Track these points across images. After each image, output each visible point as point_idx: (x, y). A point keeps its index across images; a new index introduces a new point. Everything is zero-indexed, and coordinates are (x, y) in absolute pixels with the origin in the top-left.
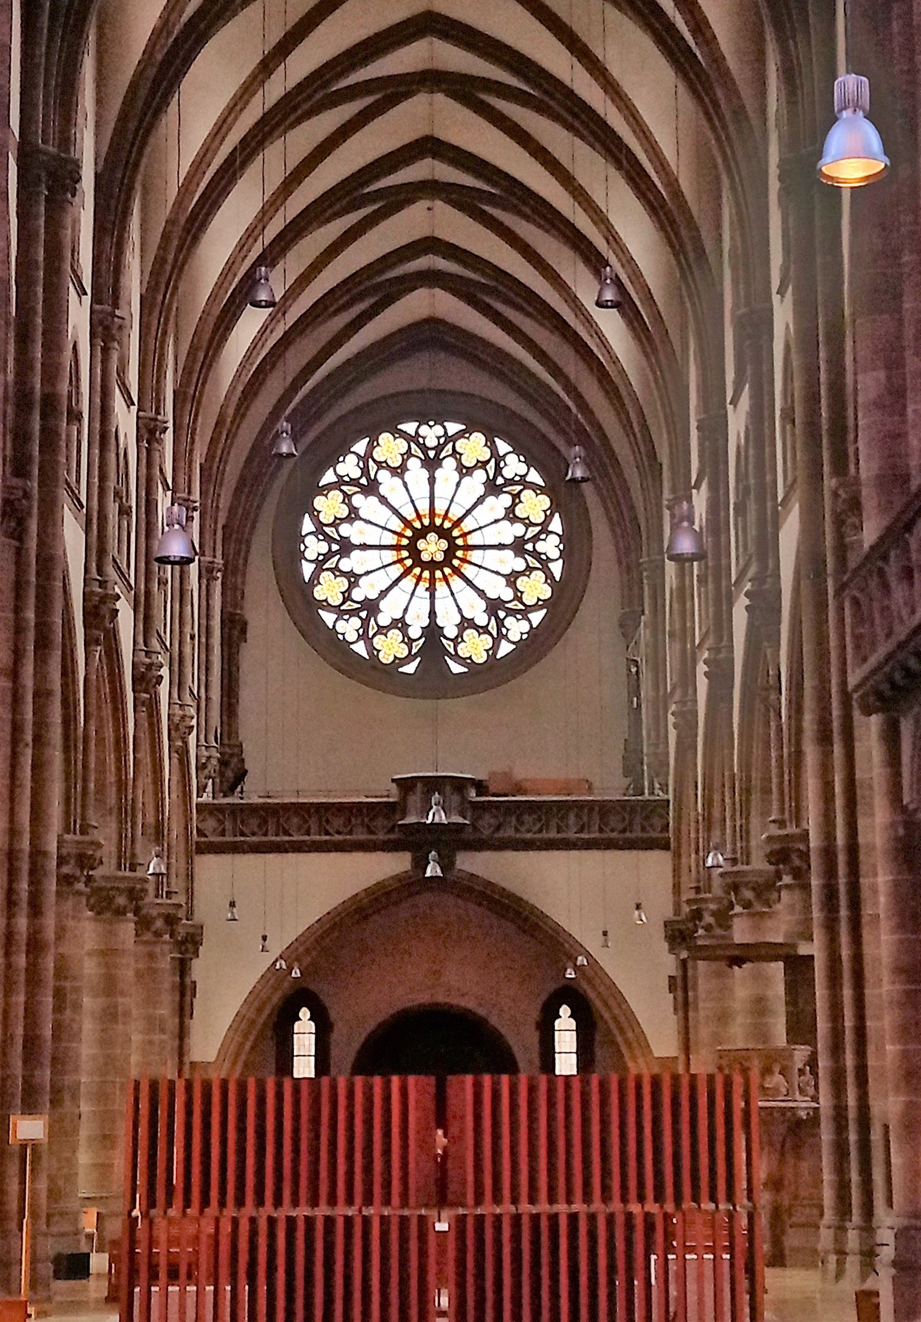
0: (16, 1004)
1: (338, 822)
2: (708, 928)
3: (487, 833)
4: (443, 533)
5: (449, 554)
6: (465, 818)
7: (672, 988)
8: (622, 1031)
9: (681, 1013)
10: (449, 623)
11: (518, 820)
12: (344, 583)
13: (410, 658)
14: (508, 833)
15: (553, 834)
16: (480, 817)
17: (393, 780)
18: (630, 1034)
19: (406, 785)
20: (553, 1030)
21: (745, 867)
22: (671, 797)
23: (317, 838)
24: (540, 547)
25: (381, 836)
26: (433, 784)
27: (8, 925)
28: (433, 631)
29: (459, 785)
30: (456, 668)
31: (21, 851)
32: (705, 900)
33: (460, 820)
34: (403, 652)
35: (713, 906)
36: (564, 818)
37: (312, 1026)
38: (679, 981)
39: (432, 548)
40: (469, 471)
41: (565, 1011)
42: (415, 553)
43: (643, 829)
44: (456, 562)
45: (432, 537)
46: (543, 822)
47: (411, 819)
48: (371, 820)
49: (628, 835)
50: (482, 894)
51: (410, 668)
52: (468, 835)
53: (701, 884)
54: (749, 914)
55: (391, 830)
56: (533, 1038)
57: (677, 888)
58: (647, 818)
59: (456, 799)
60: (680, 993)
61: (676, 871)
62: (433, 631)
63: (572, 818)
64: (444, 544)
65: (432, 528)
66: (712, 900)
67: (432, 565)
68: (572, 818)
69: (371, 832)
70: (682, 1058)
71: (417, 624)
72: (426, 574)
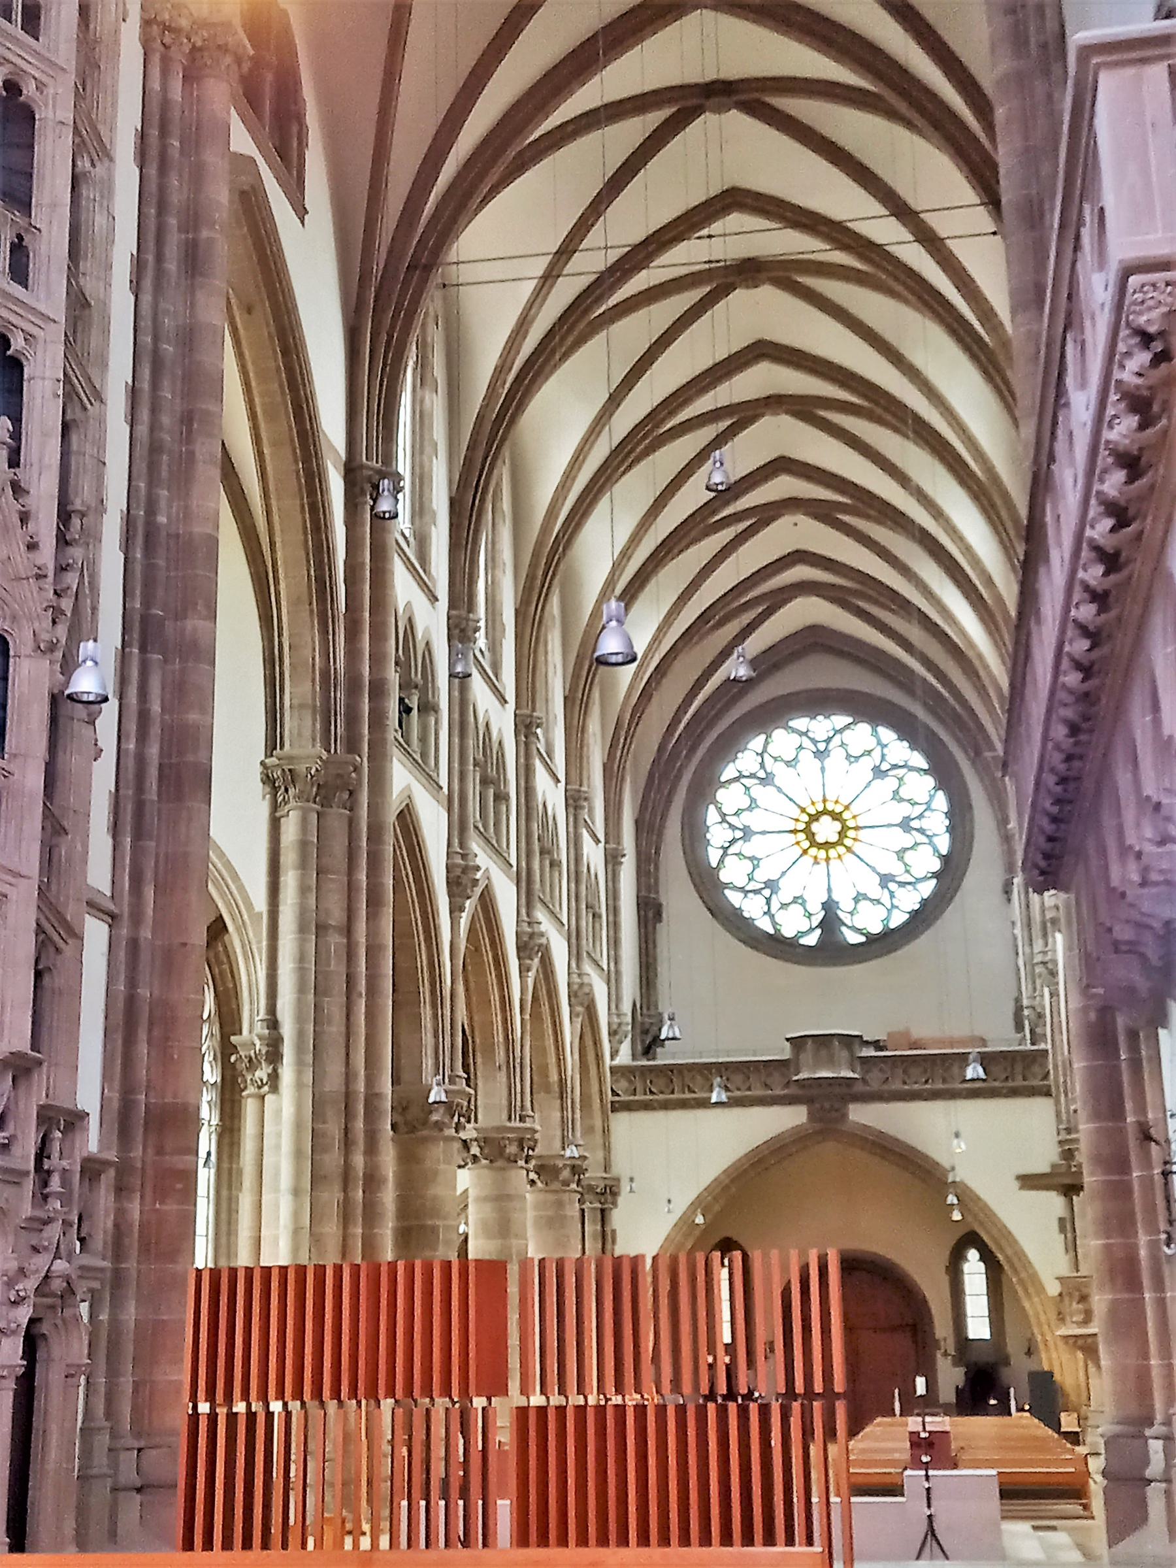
3: (875, 1085)
11: (905, 1072)
14: (896, 1085)
15: (940, 1086)
16: (867, 1072)
17: (788, 1040)
19: (797, 1043)
25: (779, 1092)
26: (823, 1041)
29: (848, 1041)
33: (851, 1075)
36: (947, 1069)
46: (928, 1075)
47: (803, 1075)
48: (770, 1075)
50: (874, 1143)
52: (859, 1088)
55: (788, 1084)
59: (845, 1054)
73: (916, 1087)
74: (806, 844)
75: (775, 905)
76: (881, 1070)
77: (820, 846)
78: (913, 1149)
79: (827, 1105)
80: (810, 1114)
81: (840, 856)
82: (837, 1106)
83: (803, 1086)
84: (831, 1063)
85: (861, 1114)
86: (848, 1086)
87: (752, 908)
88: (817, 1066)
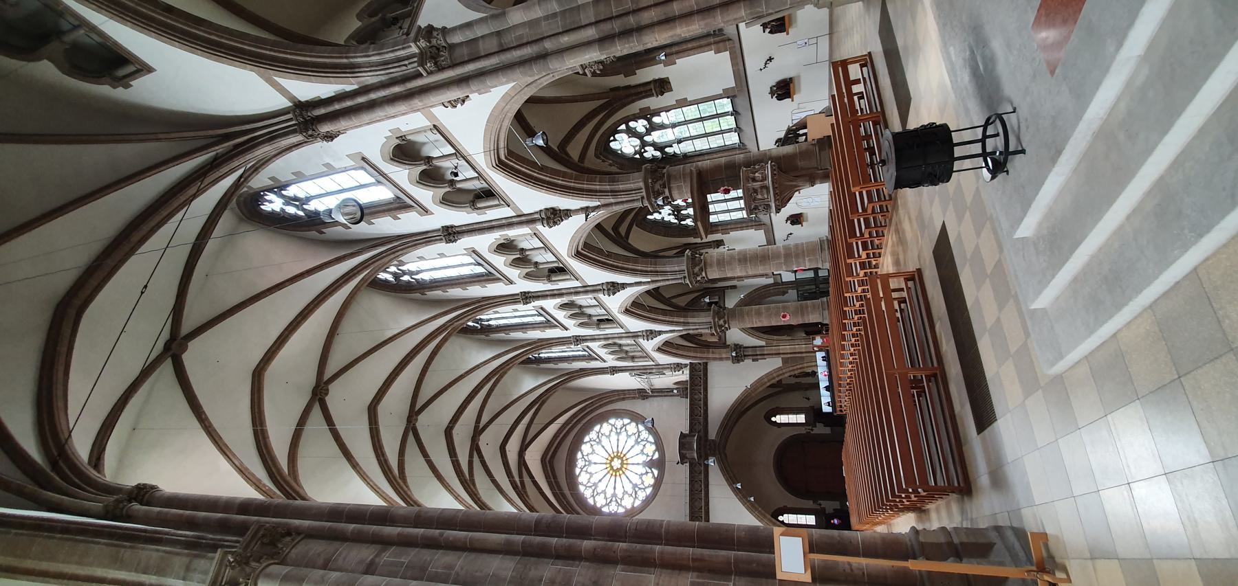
0: (662, 553)
1: (697, 486)
2: (725, 322)
4: (612, 459)
5: (618, 457)
6: (695, 436)
7: (757, 360)
8: (774, 378)
9: (765, 357)
10: (642, 458)
12: (626, 496)
13: (652, 472)
18: (775, 375)
19: (683, 458)
20: (781, 423)
21: (686, 272)
22: (687, 362)
23: (703, 495)
24: (619, 427)
27: (587, 559)
28: (646, 464)
29: (682, 436)
30: (656, 456)
31: (523, 542)
32: (714, 323)
34: (650, 475)
35: (716, 320)
36: (696, 400)
37: (785, 515)
38: (754, 357)
39: (616, 464)
40: (593, 450)
41: (773, 419)
42: (618, 470)
43: (700, 371)
44: (622, 456)
45: (613, 464)
48: (696, 472)
49: (702, 377)
51: (656, 472)
52: (702, 434)
53: (709, 326)
54: (706, 269)
56: (783, 428)
57: (721, 359)
58: (696, 370)
60: (759, 357)
61: (715, 359)
62: (646, 464)
63: (696, 397)
64: (616, 459)
65: (610, 463)
66: (714, 319)
67: (622, 464)
68: (696, 397)
69: (700, 473)
70: (782, 356)
71: (642, 470)
72: (625, 466)
73: (702, 411)
74: (621, 472)
75: (642, 486)
76: (695, 424)
77: (622, 467)
78: (727, 414)
79: (708, 447)
80: (713, 455)
81: (627, 459)
82: (708, 443)
83: (701, 457)
84: (691, 444)
85: (713, 434)
86: (701, 437)
87: (642, 495)
88: (692, 449)
